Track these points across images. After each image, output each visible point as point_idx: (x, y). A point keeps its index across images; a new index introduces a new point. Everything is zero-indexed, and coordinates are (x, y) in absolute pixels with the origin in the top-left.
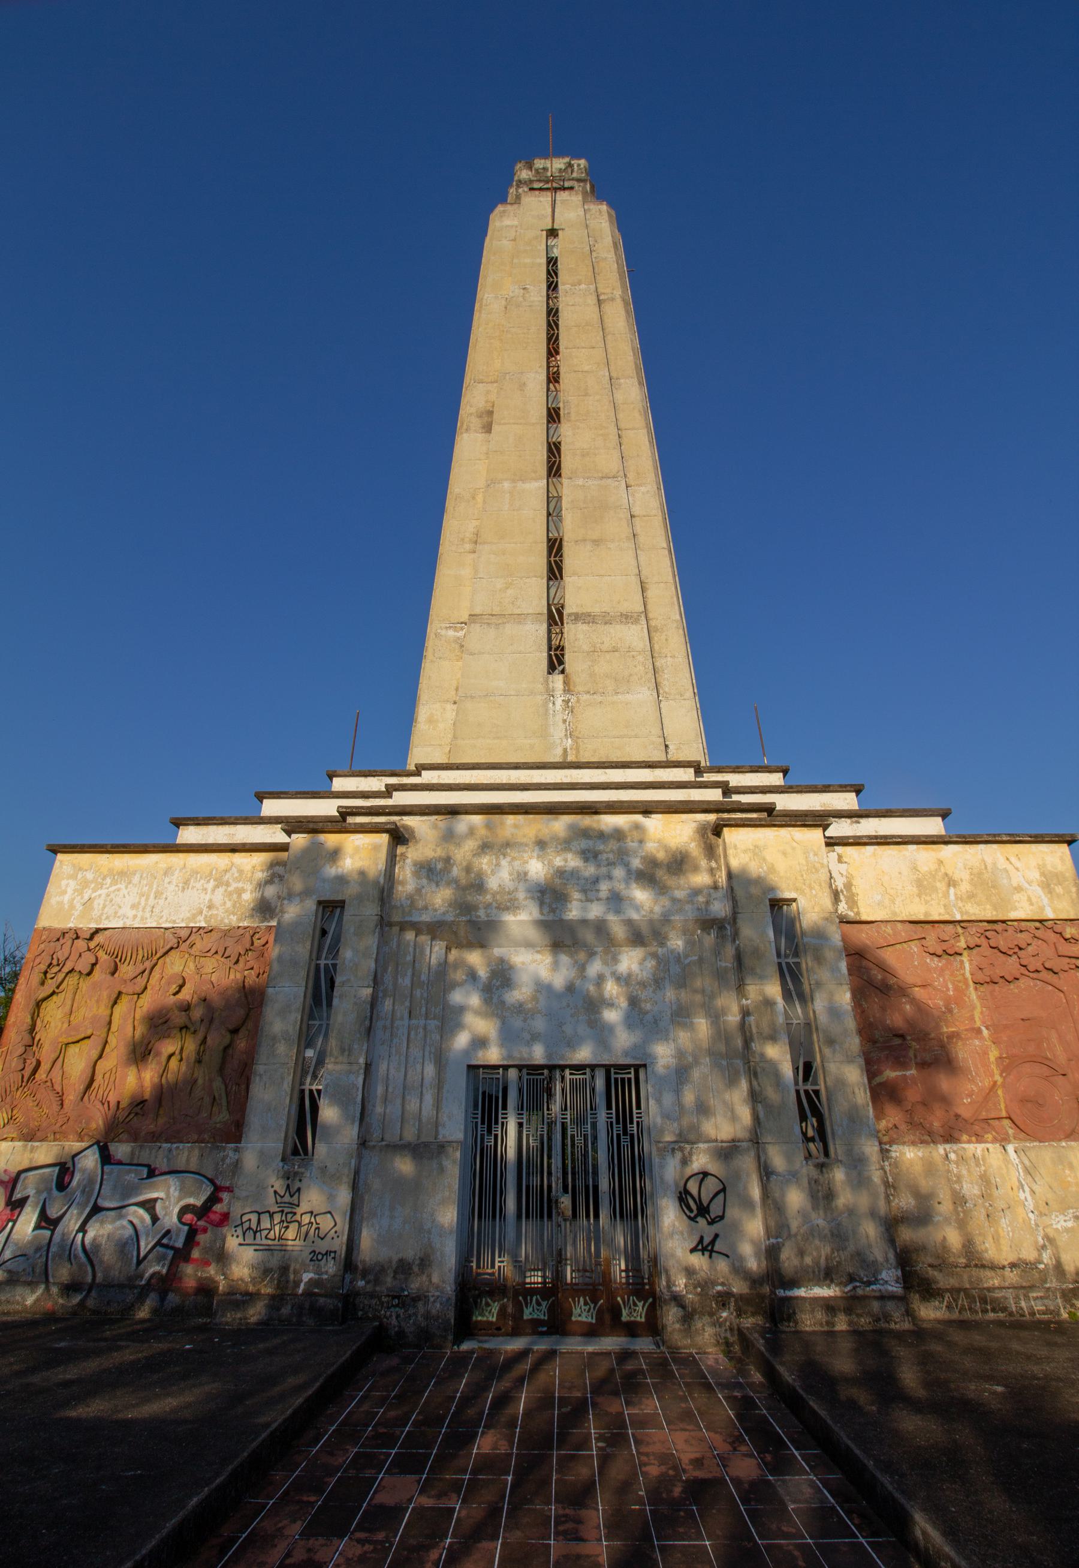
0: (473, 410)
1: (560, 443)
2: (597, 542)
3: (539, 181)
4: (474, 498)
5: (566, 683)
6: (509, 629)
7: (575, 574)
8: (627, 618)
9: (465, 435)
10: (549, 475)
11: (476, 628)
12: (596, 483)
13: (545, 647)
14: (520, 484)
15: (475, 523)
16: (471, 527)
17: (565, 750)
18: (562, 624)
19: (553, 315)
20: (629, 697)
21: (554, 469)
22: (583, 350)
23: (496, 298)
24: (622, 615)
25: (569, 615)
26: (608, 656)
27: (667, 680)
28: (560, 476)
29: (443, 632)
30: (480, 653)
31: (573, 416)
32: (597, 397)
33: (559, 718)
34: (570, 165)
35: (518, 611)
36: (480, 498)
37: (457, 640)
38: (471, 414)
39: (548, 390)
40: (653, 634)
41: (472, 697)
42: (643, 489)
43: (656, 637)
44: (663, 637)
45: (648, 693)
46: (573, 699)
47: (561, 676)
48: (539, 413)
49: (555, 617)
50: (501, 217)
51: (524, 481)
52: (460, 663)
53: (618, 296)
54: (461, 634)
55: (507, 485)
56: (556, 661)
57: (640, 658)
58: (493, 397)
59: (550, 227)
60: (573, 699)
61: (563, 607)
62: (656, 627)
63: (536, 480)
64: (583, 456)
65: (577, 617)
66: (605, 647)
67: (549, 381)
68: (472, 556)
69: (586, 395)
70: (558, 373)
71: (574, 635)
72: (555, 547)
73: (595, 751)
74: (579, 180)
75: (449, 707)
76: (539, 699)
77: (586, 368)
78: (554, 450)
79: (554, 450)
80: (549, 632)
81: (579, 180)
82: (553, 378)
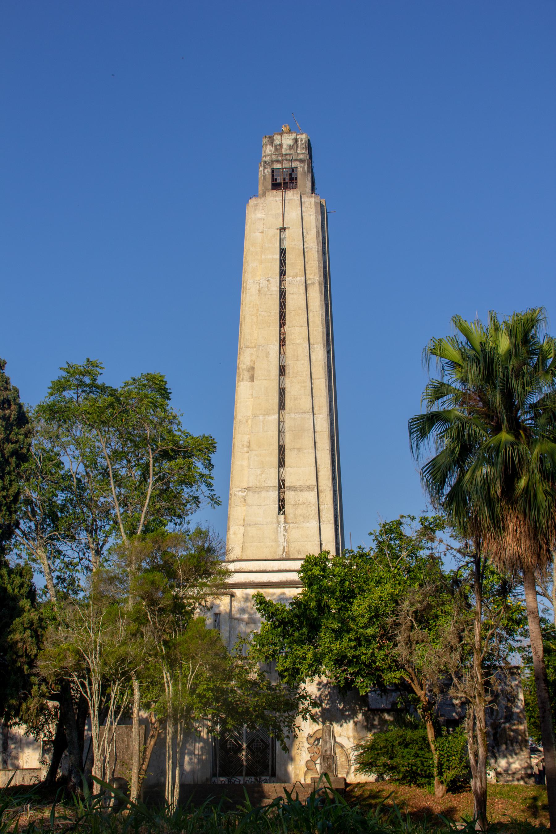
0: (245, 367)
1: (285, 389)
2: (299, 449)
3: (277, 161)
4: (247, 422)
5: (285, 519)
6: (263, 494)
7: (289, 466)
8: (309, 488)
9: (242, 383)
10: (279, 409)
11: (250, 493)
12: (300, 416)
13: (277, 502)
14: (267, 417)
15: (248, 436)
16: (246, 438)
17: (284, 547)
18: (284, 488)
19: (282, 294)
20: (308, 525)
21: (282, 405)
22: (297, 328)
23: (254, 283)
24: (307, 487)
25: (287, 487)
26: (301, 506)
27: (323, 518)
28: (285, 409)
29: (237, 493)
30: (252, 505)
31: (291, 374)
32: (302, 362)
33: (282, 533)
34: (296, 141)
35: (266, 485)
36: (250, 422)
37: (243, 497)
38: (244, 369)
39: (280, 353)
40: (320, 494)
41: (250, 525)
42: (321, 416)
43: (321, 495)
44: (324, 495)
45: (316, 523)
46: (287, 526)
47: (283, 516)
48: (275, 371)
49: (281, 485)
50: (255, 210)
51: (268, 415)
52: (245, 508)
53: (317, 281)
54: (244, 494)
55: (261, 417)
56: (281, 507)
57: (313, 507)
58: (254, 358)
59: (282, 227)
60: (287, 526)
61: (284, 480)
62: (321, 490)
63: (273, 414)
64: (295, 400)
65: (290, 488)
66: (300, 502)
67: (280, 346)
68: (248, 454)
69: (297, 360)
70: (284, 338)
71: (289, 496)
72: (282, 449)
73: (295, 548)
74: (301, 161)
75: (242, 528)
76: (275, 526)
77: (298, 342)
78: (282, 392)
79: (282, 392)
80: (279, 493)
81: (301, 161)
82: (282, 342)
